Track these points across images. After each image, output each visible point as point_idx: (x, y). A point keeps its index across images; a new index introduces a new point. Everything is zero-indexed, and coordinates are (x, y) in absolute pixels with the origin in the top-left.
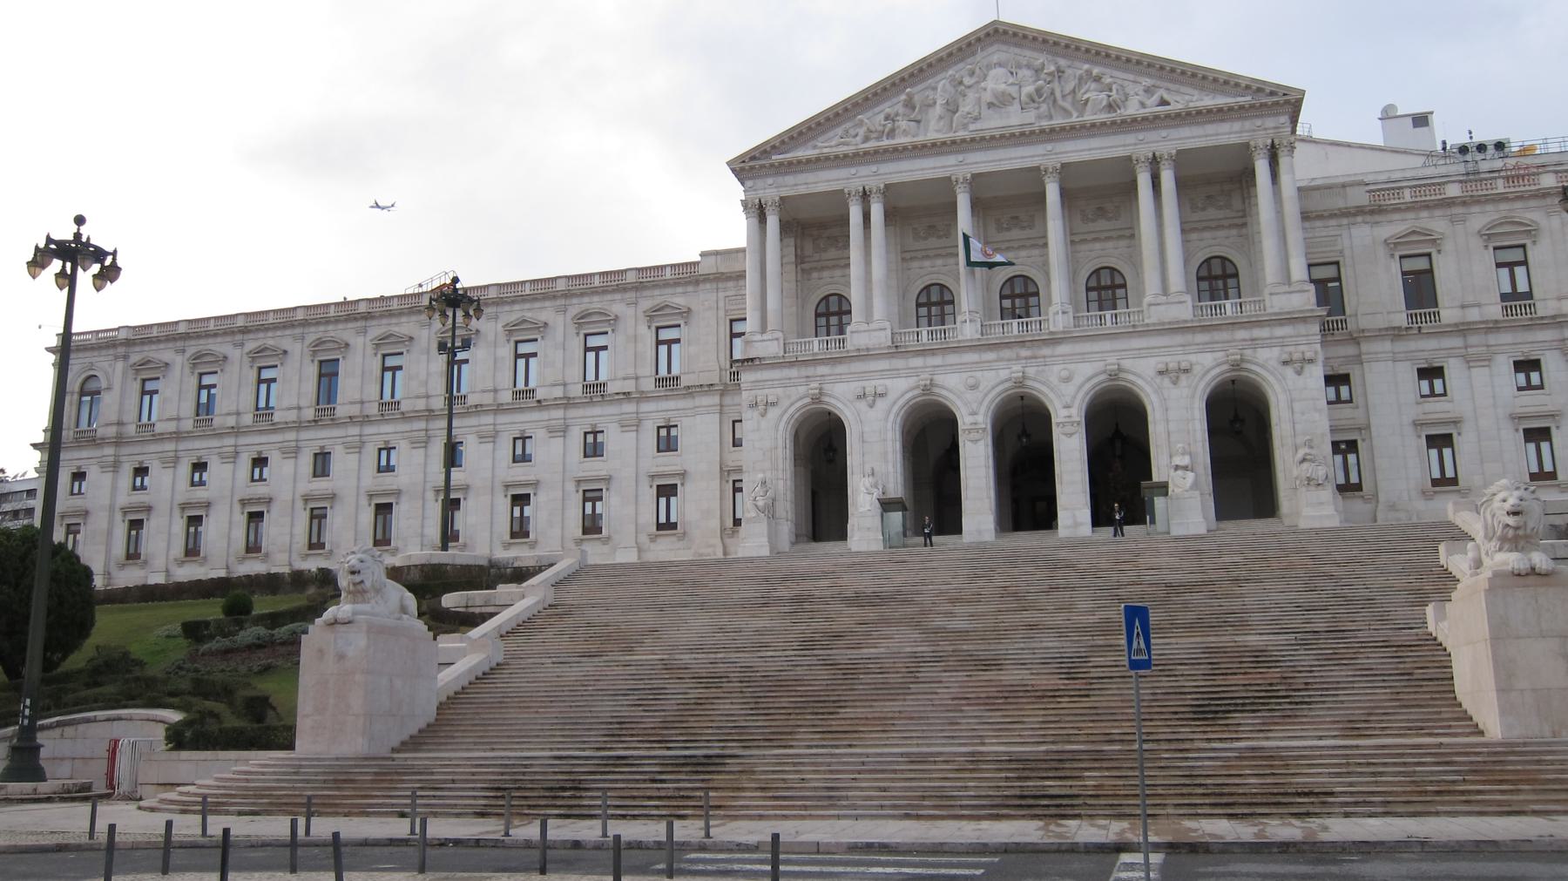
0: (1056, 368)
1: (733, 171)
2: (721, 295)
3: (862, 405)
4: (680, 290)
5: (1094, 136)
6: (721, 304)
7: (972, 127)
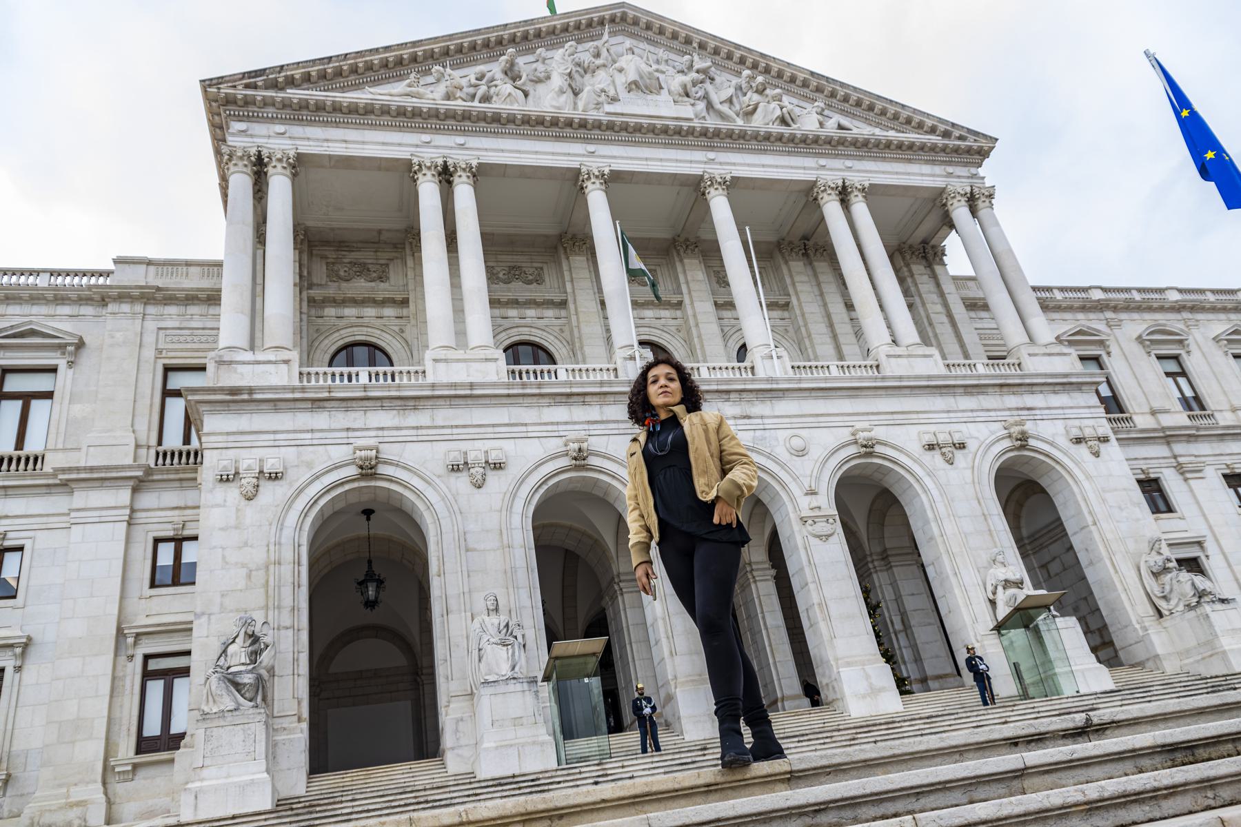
0: (782, 435)
1: (209, 99)
2: (151, 325)
3: (461, 483)
4: (66, 310)
5: (765, 151)
6: (149, 339)
7: (609, 108)
